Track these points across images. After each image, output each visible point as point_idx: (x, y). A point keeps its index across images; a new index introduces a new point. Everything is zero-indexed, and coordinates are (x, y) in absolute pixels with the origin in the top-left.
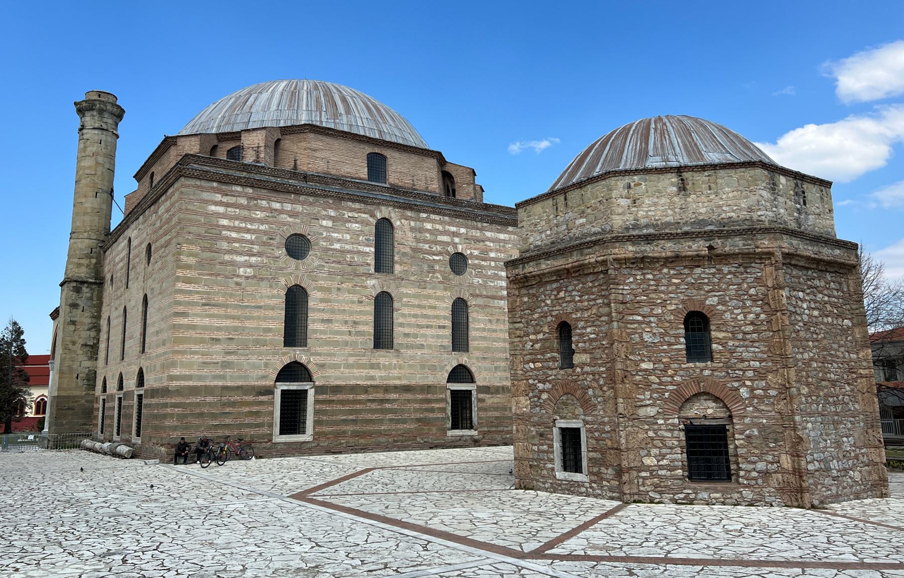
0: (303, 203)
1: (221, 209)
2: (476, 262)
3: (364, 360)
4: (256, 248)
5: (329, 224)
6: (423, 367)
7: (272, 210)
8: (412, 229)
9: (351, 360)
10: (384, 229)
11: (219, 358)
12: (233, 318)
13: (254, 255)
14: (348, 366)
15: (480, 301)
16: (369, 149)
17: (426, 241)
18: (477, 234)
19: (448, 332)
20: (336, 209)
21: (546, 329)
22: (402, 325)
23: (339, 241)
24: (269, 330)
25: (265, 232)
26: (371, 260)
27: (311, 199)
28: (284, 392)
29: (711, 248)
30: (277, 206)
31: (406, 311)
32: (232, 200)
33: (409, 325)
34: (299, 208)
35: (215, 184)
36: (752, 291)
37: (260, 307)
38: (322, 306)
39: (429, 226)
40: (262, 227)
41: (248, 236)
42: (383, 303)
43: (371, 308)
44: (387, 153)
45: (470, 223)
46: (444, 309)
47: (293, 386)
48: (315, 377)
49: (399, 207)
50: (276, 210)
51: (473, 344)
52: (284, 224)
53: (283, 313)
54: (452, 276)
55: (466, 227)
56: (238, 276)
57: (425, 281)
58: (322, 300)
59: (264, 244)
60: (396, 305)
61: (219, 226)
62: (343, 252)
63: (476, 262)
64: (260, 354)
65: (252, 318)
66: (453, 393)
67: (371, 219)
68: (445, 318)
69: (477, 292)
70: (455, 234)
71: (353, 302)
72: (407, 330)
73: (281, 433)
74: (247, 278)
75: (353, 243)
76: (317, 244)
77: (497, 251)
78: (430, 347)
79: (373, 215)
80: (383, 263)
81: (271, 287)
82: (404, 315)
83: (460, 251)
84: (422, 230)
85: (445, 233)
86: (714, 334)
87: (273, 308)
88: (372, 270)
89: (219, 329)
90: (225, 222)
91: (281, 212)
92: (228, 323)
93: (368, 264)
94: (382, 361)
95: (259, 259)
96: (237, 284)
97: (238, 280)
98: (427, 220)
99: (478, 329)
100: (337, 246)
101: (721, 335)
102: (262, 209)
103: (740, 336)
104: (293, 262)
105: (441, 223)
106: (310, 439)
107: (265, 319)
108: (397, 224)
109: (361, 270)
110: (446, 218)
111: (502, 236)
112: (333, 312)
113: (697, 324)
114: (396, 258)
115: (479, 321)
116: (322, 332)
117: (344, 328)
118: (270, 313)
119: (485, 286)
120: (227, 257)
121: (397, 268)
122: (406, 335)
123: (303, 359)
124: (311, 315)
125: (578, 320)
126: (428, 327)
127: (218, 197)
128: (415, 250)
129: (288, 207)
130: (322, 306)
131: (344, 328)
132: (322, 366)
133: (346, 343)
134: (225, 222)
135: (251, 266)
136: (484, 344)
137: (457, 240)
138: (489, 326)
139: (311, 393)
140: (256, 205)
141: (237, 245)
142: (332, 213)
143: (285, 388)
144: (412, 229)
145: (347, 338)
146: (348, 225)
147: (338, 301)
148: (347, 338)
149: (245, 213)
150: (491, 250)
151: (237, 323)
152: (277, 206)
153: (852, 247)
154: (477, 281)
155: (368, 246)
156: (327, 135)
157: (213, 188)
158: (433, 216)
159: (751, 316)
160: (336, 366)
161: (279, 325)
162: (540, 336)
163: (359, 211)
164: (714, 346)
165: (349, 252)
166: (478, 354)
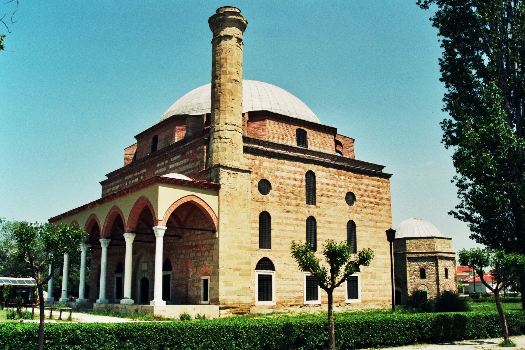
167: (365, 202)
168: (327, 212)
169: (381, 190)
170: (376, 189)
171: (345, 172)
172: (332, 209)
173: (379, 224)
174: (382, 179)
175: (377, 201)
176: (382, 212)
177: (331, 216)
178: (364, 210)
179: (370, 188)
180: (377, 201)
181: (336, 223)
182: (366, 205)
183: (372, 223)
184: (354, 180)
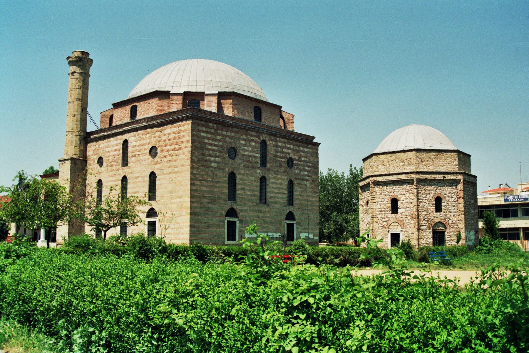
0: (234, 132)
1: (205, 135)
2: (297, 162)
3: (256, 209)
4: (218, 154)
6: (277, 212)
7: (223, 135)
8: (274, 146)
9: (252, 208)
10: (264, 143)
12: (210, 186)
13: (217, 157)
14: (251, 211)
16: (255, 104)
18: (297, 148)
19: (285, 196)
20: (246, 136)
21: (387, 200)
22: (270, 192)
23: (247, 151)
24: (222, 193)
25: (221, 146)
26: (258, 161)
27: (237, 130)
29: (444, 177)
30: (225, 133)
31: (271, 185)
32: (209, 130)
33: (272, 192)
34: (233, 134)
35: (203, 123)
37: (219, 182)
38: (241, 182)
39: (280, 144)
40: (220, 144)
41: (215, 148)
42: (263, 180)
43: (258, 184)
45: (295, 143)
46: (285, 184)
47: (232, 219)
51: (295, 202)
52: (227, 142)
55: (293, 145)
56: (212, 167)
57: (278, 171)
58: (242, 180)
59: (220, 152)
60: (268, 183)
61: (204, 143)
62: (249, 156)
63: (297, 162)
66: (288, 224)
68: (285, 189)
70: (290, 148)
71: (252, 181)
72: (271, 195)
73: (228, 240)
74: (215, 168)
75: (252, 152)
77: (305, 157)
79: (259, 139)
80: (264, 162)
82: (270, 188)
84: (276, 146)
86: (442, 204)
87: (224, 183)
90: (206, 141)
92: (208, 189)
93: (258, 162)
96: (212, 171)
97: (211, 169)
98: (279, 141)
99: (297, 195)
100: (246, 153)
102: (220, 135)
104: (231, 161)
105: (284, 143)
107: (222, 188)
108: (268, 143)
109: (255, 165)
111: (307, 150)
112: (245, 185)
113: (438, 201)
114: (268, 160)
117: (249, 193)
118: (223, 185)
119: (299, 174)
120: (208, 158)
122: (271, 197)
123: (235, 207)
124: (238, 187)
125: (400, 198)
126: (279, 193)
127: (204, 129)
128: (275, 156)
129: (229, 134)
130: (241, 182)
132: (241, 210)
133: (250, 200)
134: (206, 141)
135: (216, 162)
136: (299, 202)
137: (290, 151)
138: (301, 194)
139: (237, 222)
140: (217, 133)
141: (211, 152)
142: (245, 137)
144: (274, 146)
145: (250, 198)
146: (251, 143)
148: (250, 198)
149: (213, 137)
152: (225, 133)
154: (297, 171)
156: (239, 97)
157: (202, 124)
160: (246, 211)
161: (226, 191)
162: (384, 202)
163: (254, 136)
164: (442, 208)
165: (251, 156)
167: (166, 151)
168: (135, 169)
169: (182, 134)
170: (177, 135)
171: (150, 130)
172: (139, 166)
173: (176, 170)
174: (184, 122)
175: (177, 146)
176: (180, 157)
177: (138, 172)
178: (165, 159)
179: (171, 136)
180: (177, 146)
181: (141, 177)
182: (166, 154)
183: (170, 170)
184: (158, 134)
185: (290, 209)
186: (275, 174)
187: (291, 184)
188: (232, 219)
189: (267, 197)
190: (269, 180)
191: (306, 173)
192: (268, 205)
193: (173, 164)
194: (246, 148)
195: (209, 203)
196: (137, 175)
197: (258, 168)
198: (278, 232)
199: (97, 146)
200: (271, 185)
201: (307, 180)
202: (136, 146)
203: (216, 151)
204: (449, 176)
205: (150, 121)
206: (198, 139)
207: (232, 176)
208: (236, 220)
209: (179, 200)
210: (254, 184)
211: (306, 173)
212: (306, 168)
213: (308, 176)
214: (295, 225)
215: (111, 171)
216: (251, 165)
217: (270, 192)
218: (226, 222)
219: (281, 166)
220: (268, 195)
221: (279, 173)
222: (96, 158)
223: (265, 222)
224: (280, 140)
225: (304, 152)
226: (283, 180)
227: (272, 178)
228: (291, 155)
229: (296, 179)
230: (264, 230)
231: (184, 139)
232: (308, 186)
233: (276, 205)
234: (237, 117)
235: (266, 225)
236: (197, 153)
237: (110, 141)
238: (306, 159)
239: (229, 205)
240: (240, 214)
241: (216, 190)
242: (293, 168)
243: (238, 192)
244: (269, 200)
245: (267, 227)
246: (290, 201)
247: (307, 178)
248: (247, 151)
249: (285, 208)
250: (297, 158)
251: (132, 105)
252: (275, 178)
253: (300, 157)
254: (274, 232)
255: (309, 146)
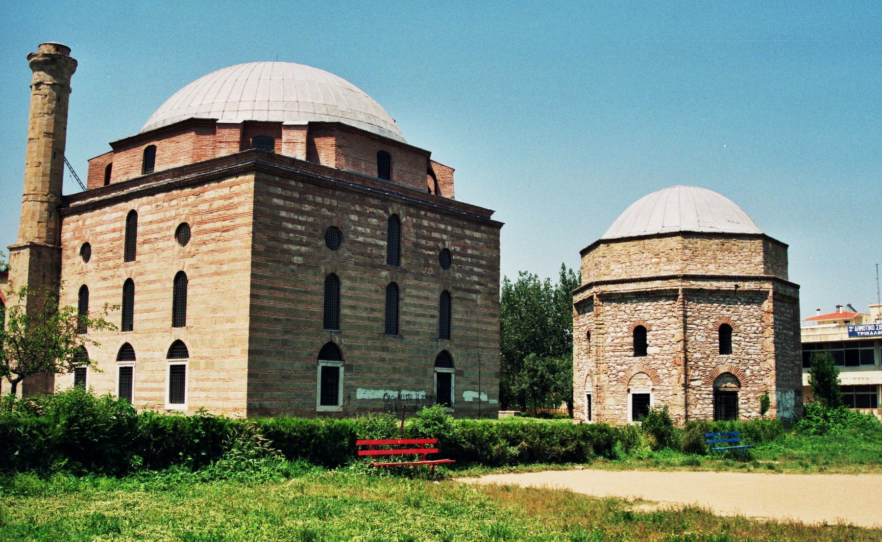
0: (338, 199)
1: (280, 202)
2: (458, 257)
3: (378, 344)
4: (305, 239)
5: (354, 217)
6: (419, 350)
9: (370, 343)
11: (280, 337)
12: (289, 300)
15: (460, 294)
16: (379, 147)
17: (424, 237)
18: (459, 231)
19: (435, 321)
21: (625, 329)
22: (405, 313)
23: (363, 234)
24: (312, 314)
25: (311, 224)
26: (384, 253)
27: (344, 194)
28: (323, 367)
29: (737, 286)
30: (319, 200)
32: (289, 193)
33: (410, 313)
34: (335, 203)
35: (277, 179)
36: (756, 314)
40: (311, 219)
41: (299, 227)
42: (393, 291)
43: (383, 297)
44: (392, 150)
45: (455, 221)
47: (331, 364)
48: (345, 357)
49: (406, 205)
50: (318, 204)
51: (454, 332)
53: (323, 297)
54: (441, 270)
55: (452, 226)
56: (294, 264)
57: (422, 274)
58: (350, 289)
59: (310, 235)
60: (401, 295)
62: (365, 244)
63: (458, 257)
64: (308, 334)
65: (302, 302)
66: (439, 374)
67: (386, 216)
68: (435, 308)
69: (458, 285)
70: (445, 232)
72: (407, 318)
73: (322, 404)
74: (299, 265)
75: (372, 237)
76: (348, 237)
77: (474, 248)
78: (424, 332)
79: (387, 212)
80: (394, 257)
81: (315, 275)
82: (406, 304)
83: (447, 246)
84: (420, 227)
85: (438, 230)
86: (733, 338)
88: (385, 263)
89: (280, 310)
90: (283, 214)
91: (322, 205)
92: (286, 306)
93: (383, 257)
94: (390, 344)
95: (307, 249)
96: (292, 271)
97: (292, 267)
98: (425, 217)
99: (457, 320)
100: (361, 239)
101: (738, 338)
102: (309, 203)
103: (748, 340)
104: (330, 254)
105: (434, 220)
106: (341, 410)
107: (311, 303)
109: (378, 262)
110: (438, 216)
111: (477, 235)
112: (358, 299)
113: (725, 332)
114: (403, 252)
115: (458, 312)
116: (350, 317)
119: (462, 280)
120: (285, 246)
121: (403, 261)
122: (408, 323)
123: (337, 340)
124: (344, 302)
125: (651, 325)
126: (423, 316)
127: (279, 191)
128: (417, 245)
129: (327, 202)
131: (364, 315)
132: (350, 348)
134: (283, 214)
135: (301, 255)
136: (461, 333)
137: (445, 237)
139: (342, 370)
140: (305, 199)
141: (292, 235)
142: (358, 208)
143: (324, 365)
146: (369, 220)
147: (361, 289)
148: (367, 323)
149: (297, 206)
150: (469, 248)
151: (292, 307)
152: (319, 200)
153: (797, 287)
154: (458, 275)
155: (382, 240)
157: (276, 182)
158: (429, 214)
159: (754, 329)
160: (359, 348)
161: (319, 309)
162: (620, 334)
164: (733, 345)
165: (370, 245)
166: (457, 342)
167: (206, 232)
168: (150, 267)
169: (236, 200)
170: (226, 203)
171: (179, 192)
172: (155, 260)
173: (225, 268)
174: (241, 178)
175: (227, 223)
176: (232, 244)
177: (153, 272)
178: (204, 248)
179: (216, 204)
180: (227, 223)
181: (159, 280)
182: (205, 237)
183: (214, 268)
184: (192, 199)
185: (445, 345)
186: (416, 279)
187: (446, 298)
188: (331, 364)
189: (400, 322)
190: (405, 290)
191: (475, 278)
192: (401, 337)
193: (218, 256)
194: (360, 229)
195: (286, 332)
196: (152, 277)
197: (383, 267)
198: (421, 390)
199: (80, 223)
200: (408, 300)
201: (476, 292)
202: (151, 222)
203: (301, 233)
204: (747, 284)
205: (178, 176)
206: (268, 211)
207: (332, 283)
208: (339, 365)
209: (229, 326)
210: (375, 296)
211: (475, 278)
212: (476, 269)
213: (479, 283)
214: (453, 376)
215: (104, 269)
216: (368, 260)
217: (405, 313)
218: (319, 369)
219: (427, 265)
220: (403, 318)
221: (424, 279)
222: (78, 244)
223: (395, 370)
224: (425, 215)
225: (472, 238)
226: (431, 290)
227: (410, 286)
228: (447, 243)
229: (457, 289)
230: (393, 384)
231: (240, 210)
232: (479, 302)
233: (416, 338)
234: (345, 169)
235: (397, 376)
236: (265, 238)
237: (105, 213)
238: (476, 253)
239: (326, 336)
240: (346, 354)
241: (301, 307)
242: (451, 269)
243: (344, 311)
244: (403, 327)
245: (399, 380)
246: (445, 331)
247: (478, 287)
248: (363, 234)
249: (434, 343)
250: (458, 249)
251: (146, 146)
252: (416, 287)
253: (464, 248)
254: (412, 390)
255: (483, 228)
